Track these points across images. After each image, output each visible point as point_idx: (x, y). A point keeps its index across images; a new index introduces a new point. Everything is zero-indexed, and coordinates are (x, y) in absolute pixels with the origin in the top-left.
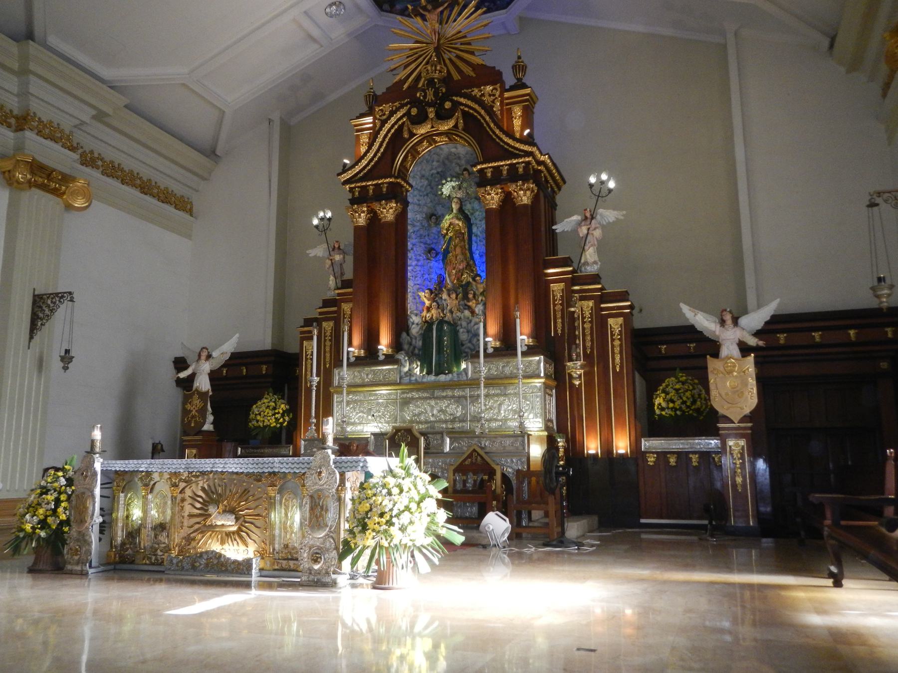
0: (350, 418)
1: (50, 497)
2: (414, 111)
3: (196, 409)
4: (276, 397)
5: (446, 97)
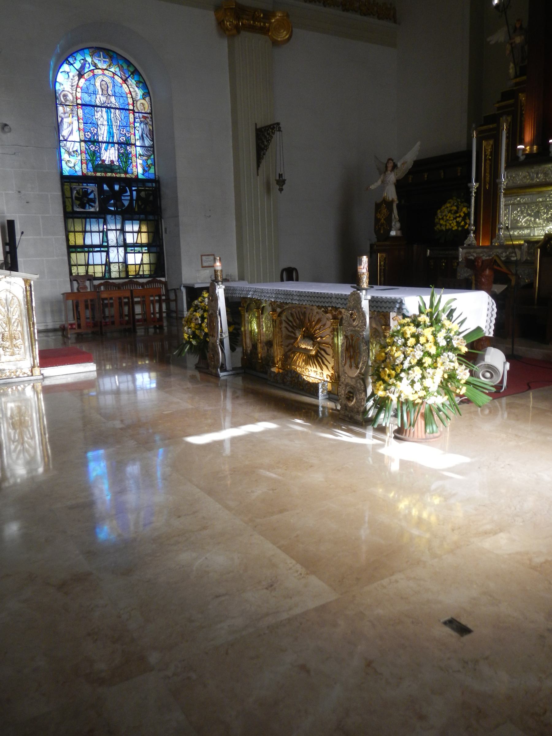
0: (518, 222)
1: (198, 315)
3: (384, 217)
4: (459, 200)
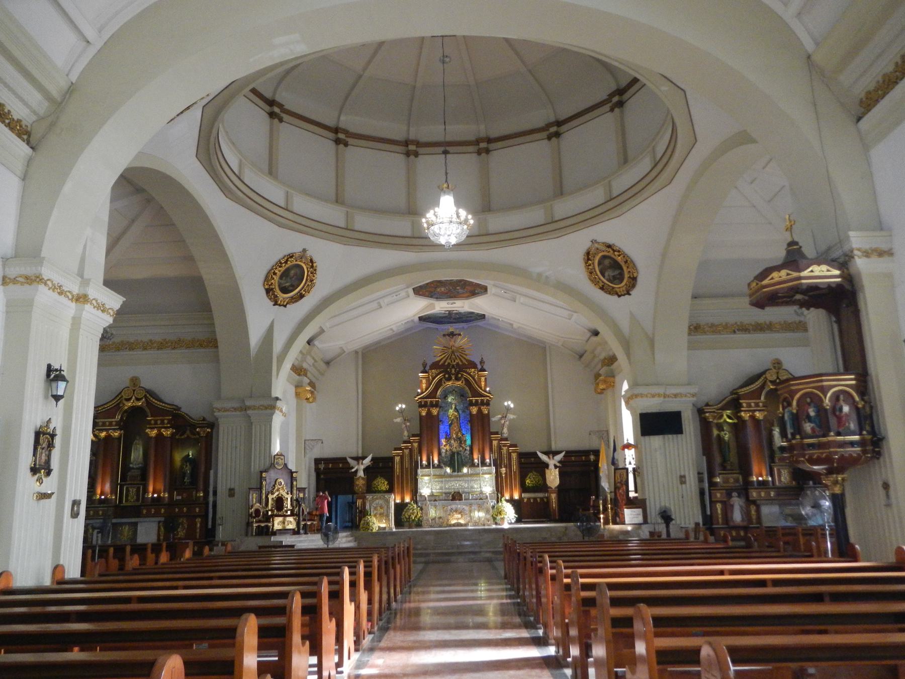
1: (415, 511)
2: (447, 376)
5: (458, 373)
